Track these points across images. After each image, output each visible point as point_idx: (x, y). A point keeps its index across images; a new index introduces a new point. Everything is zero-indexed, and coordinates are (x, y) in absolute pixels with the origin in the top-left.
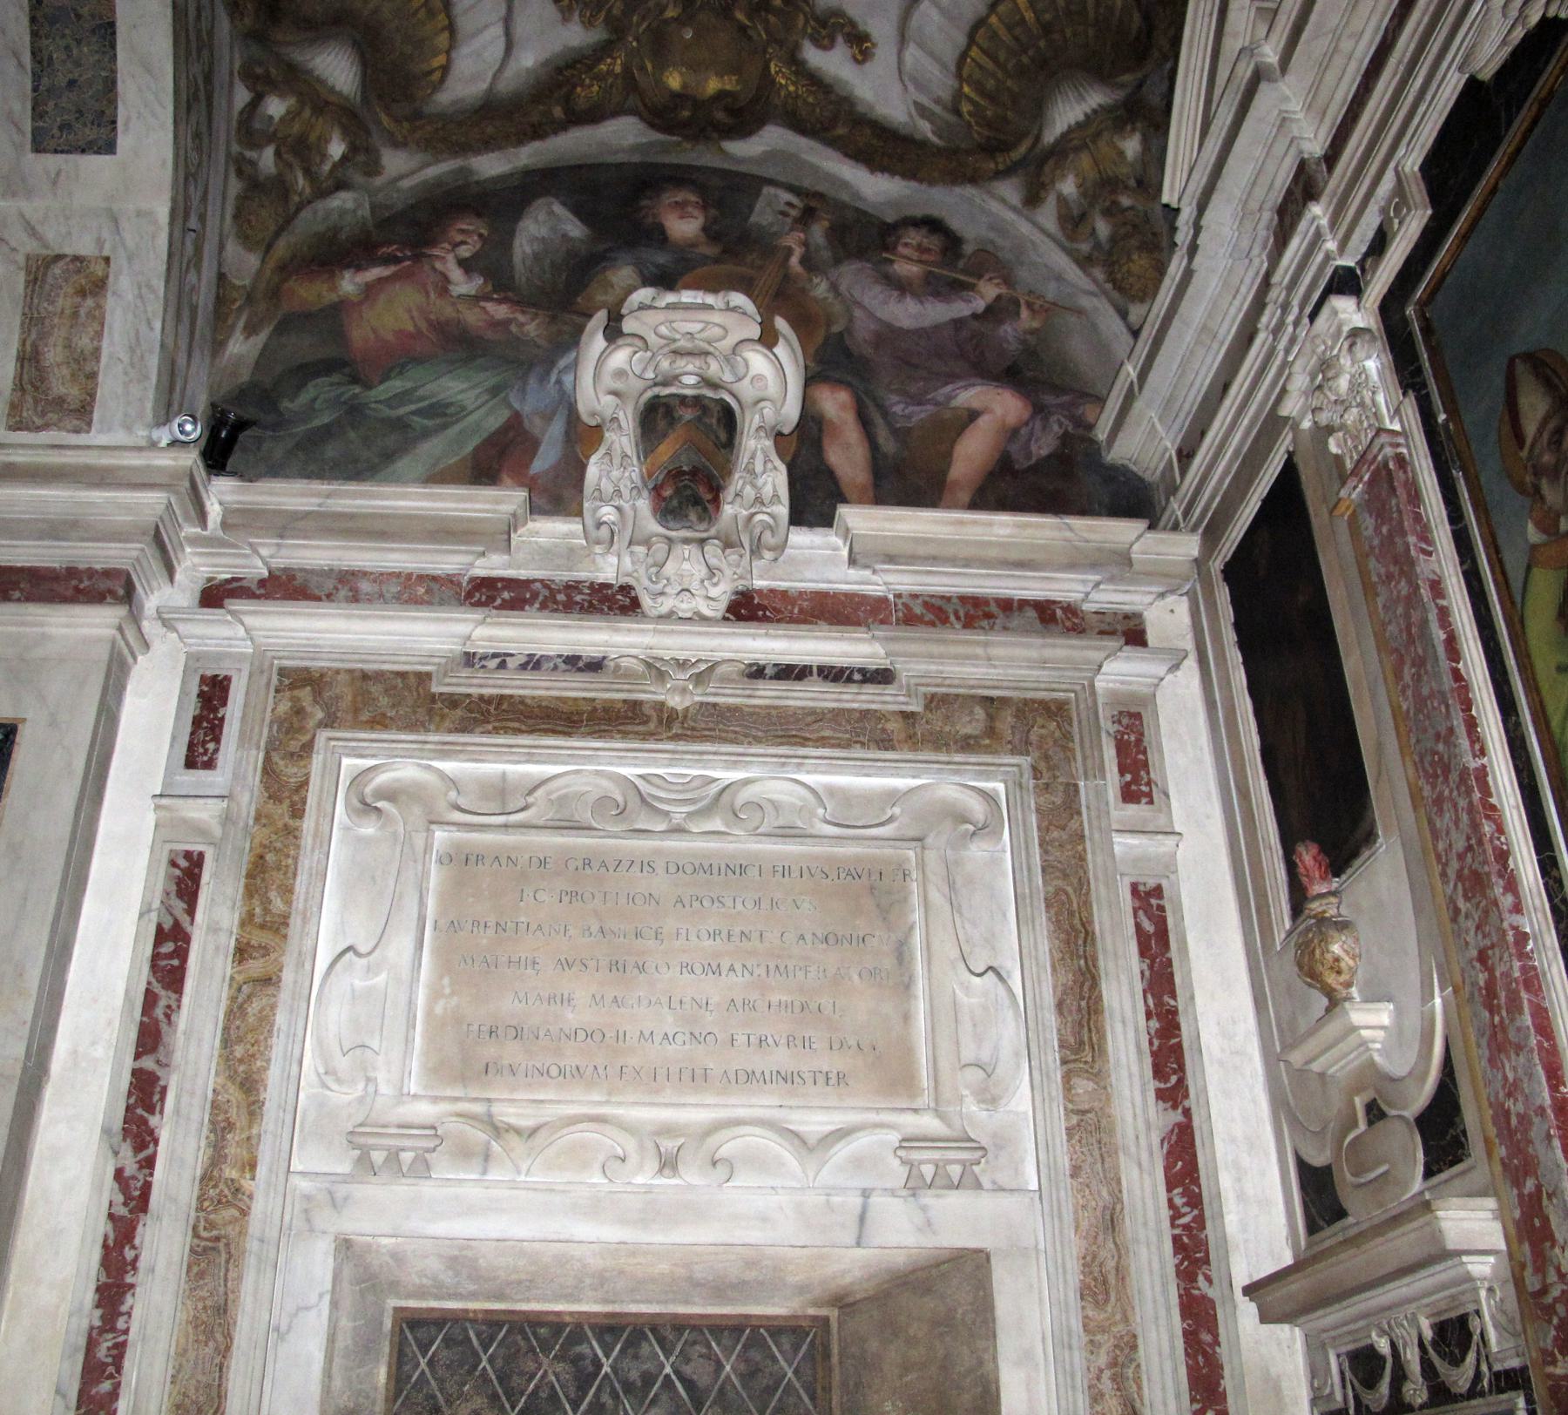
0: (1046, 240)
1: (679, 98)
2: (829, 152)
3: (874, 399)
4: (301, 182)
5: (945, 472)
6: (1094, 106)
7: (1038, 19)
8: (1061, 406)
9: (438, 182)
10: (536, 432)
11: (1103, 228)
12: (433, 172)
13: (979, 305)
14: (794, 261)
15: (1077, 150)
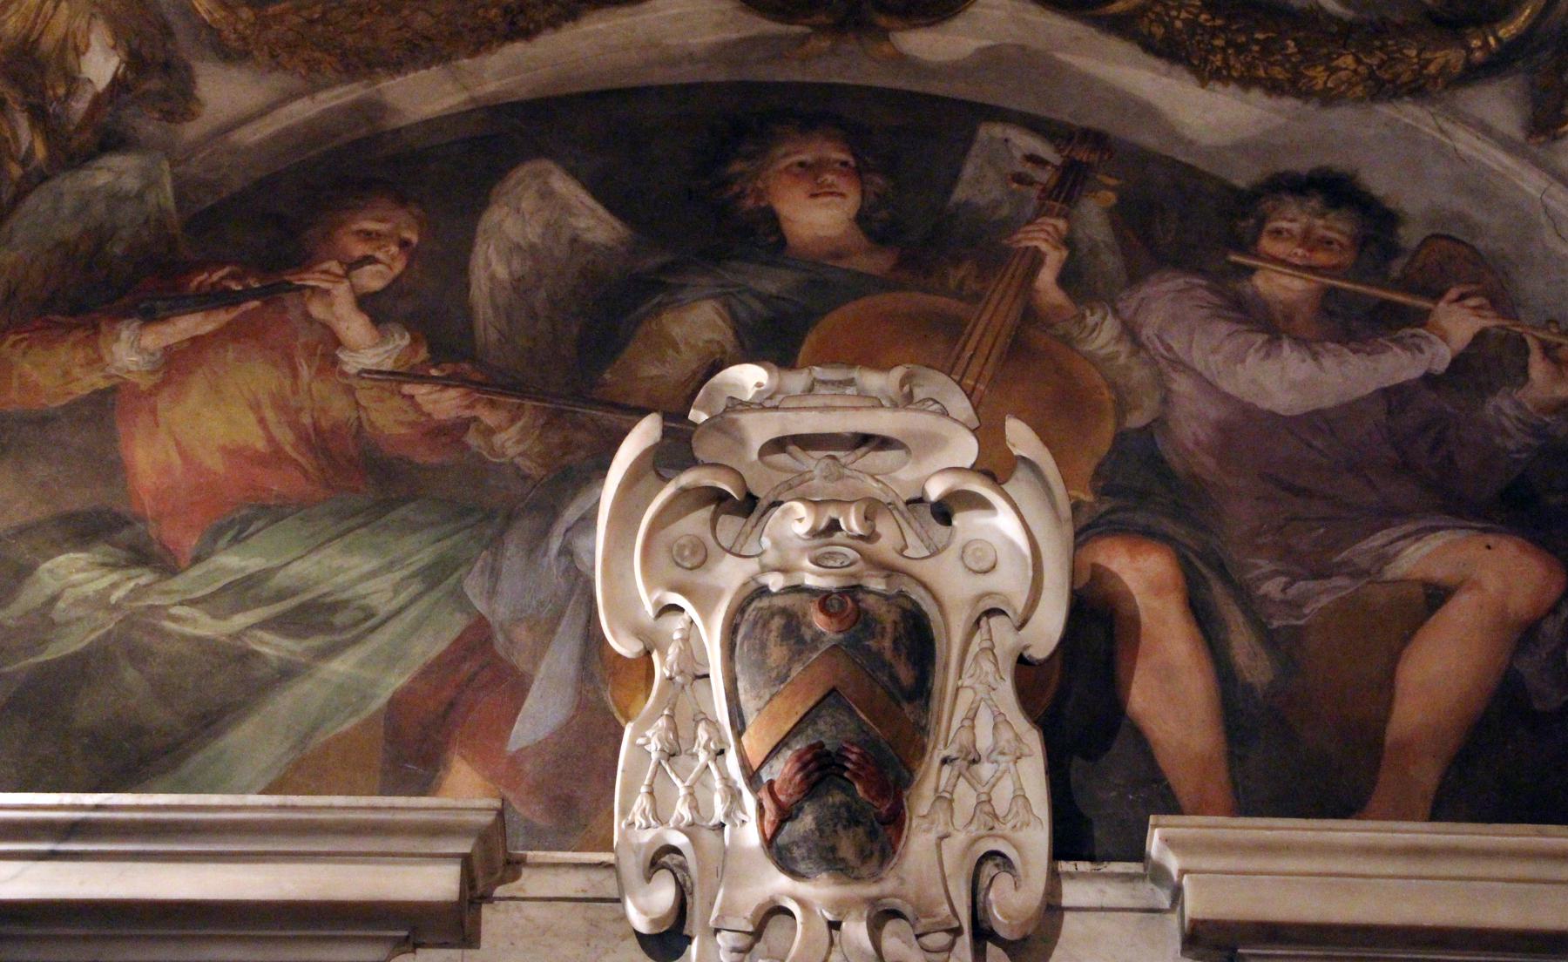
2: (1117, 46)
3: (1221, 569)
5: (1380, 732)
9: (312, 132)
10: (521, 661)
12: (302, 110)
13: (1439, 356)
14: (1046, 278)
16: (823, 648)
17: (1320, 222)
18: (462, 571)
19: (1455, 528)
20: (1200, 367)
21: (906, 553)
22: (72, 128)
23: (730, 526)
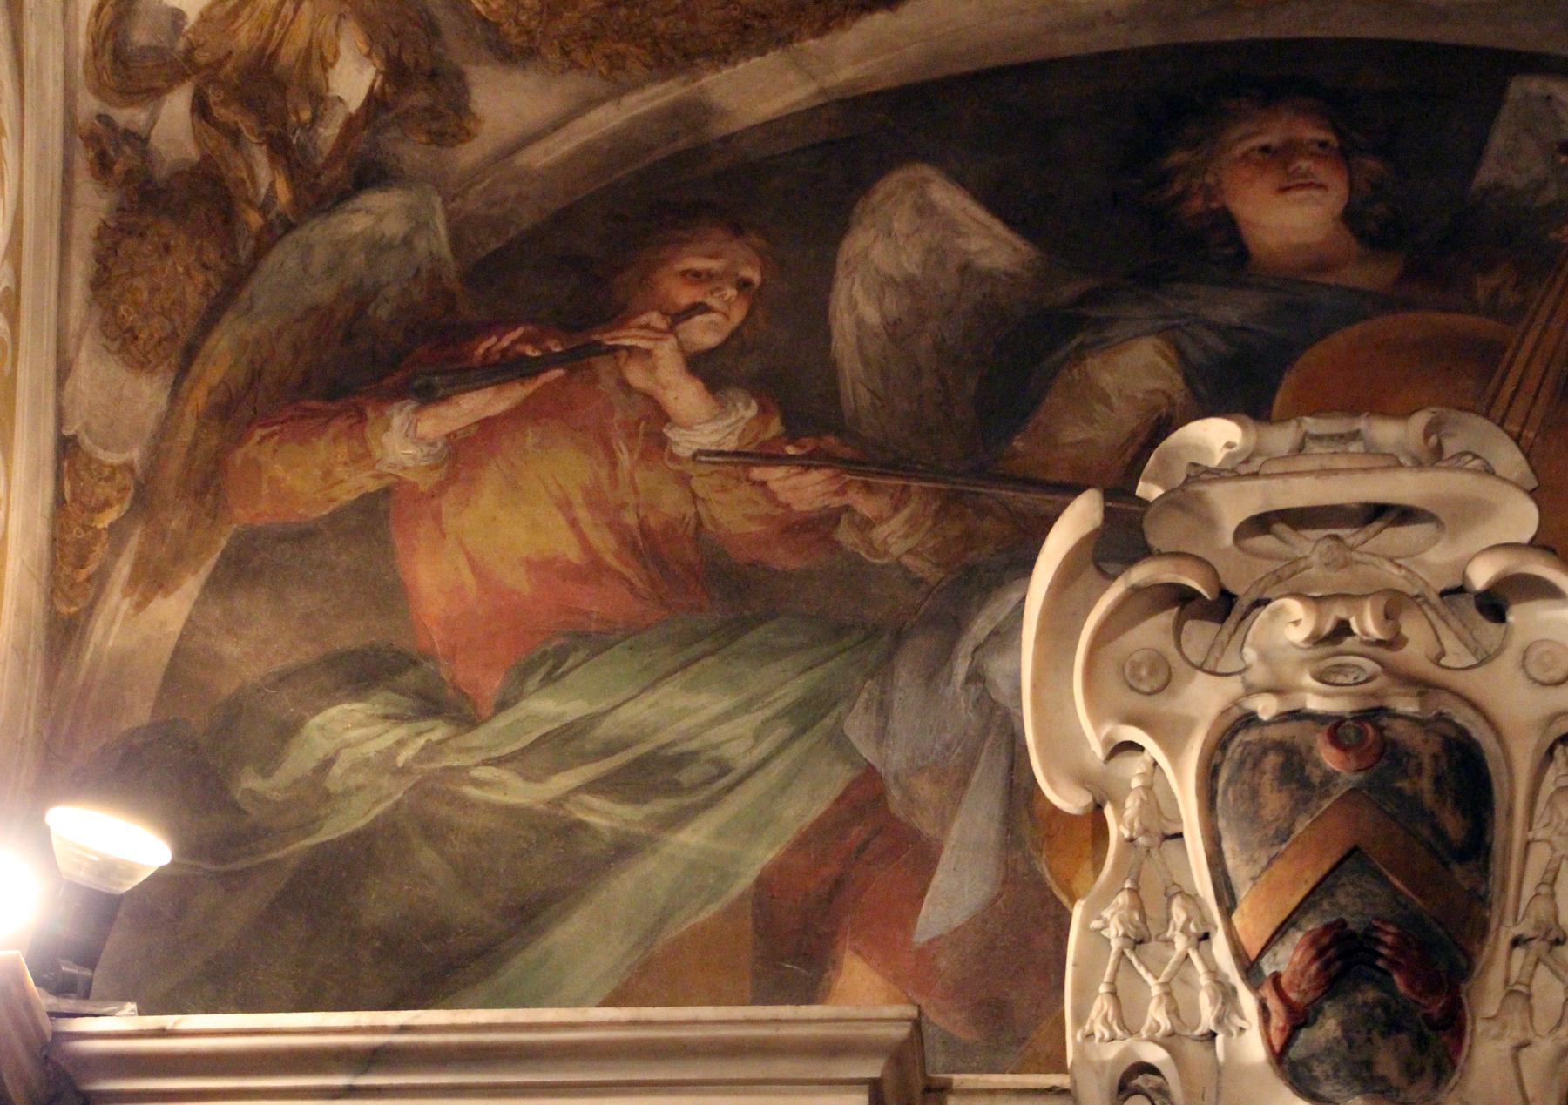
9: (620, 147)
10: (925, 823)
12: (606, 119)
16: (1337, 794)
18: (842, 708)
21: (1443, 661)
22: (320, 161)
23: (1199, 634)
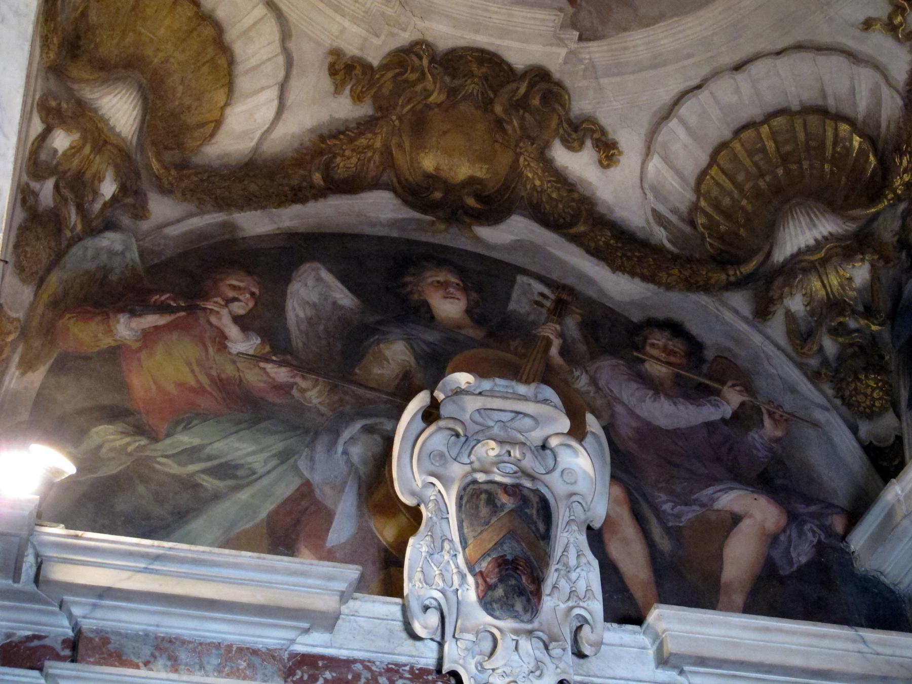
0: (778, 353)
1: (433, 179)
3: (644, 495)
4: (73, 217)
6: (825, 233)
7: (778, 148)
8: (812, 515)
9: (201, 235)
10: (329, 503)
11: (830, 346)
14: (554, 351)
15: (805, 271)
16: (506, 510)
17: (671, 343)
18: (296, 457)
19: (743, 489)
20: (626, 402)
22: (93, 216)
